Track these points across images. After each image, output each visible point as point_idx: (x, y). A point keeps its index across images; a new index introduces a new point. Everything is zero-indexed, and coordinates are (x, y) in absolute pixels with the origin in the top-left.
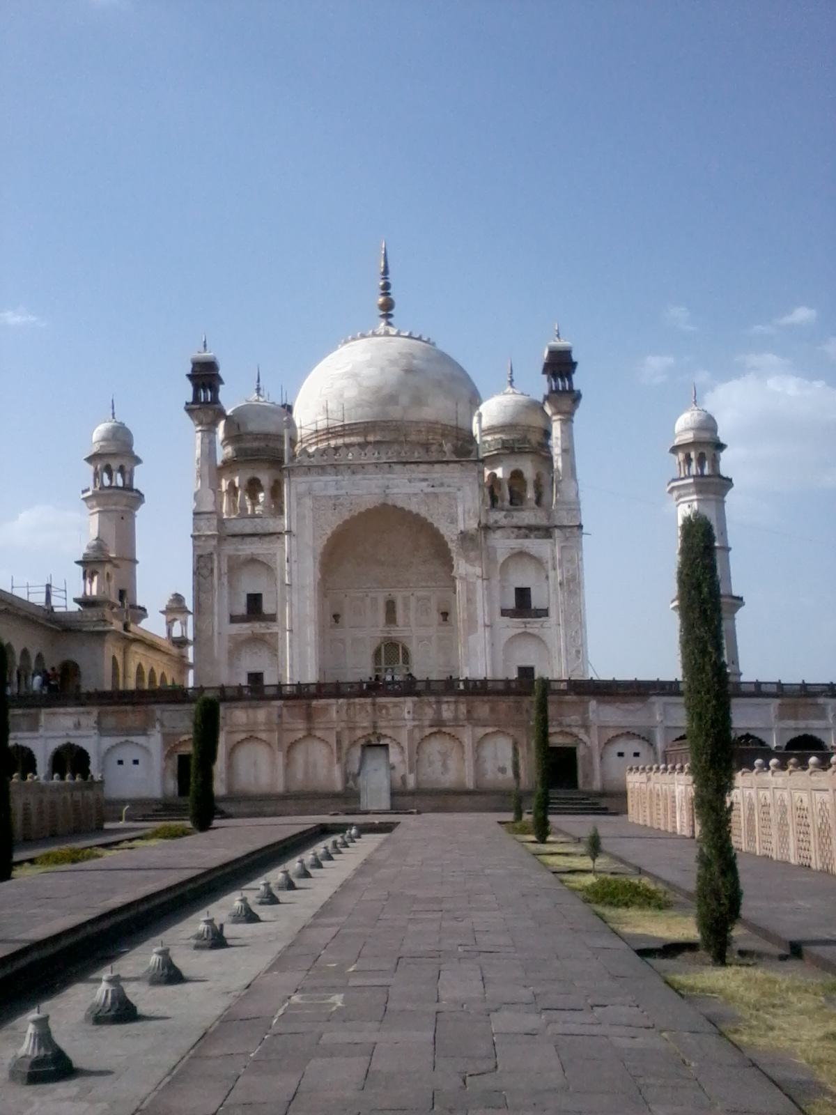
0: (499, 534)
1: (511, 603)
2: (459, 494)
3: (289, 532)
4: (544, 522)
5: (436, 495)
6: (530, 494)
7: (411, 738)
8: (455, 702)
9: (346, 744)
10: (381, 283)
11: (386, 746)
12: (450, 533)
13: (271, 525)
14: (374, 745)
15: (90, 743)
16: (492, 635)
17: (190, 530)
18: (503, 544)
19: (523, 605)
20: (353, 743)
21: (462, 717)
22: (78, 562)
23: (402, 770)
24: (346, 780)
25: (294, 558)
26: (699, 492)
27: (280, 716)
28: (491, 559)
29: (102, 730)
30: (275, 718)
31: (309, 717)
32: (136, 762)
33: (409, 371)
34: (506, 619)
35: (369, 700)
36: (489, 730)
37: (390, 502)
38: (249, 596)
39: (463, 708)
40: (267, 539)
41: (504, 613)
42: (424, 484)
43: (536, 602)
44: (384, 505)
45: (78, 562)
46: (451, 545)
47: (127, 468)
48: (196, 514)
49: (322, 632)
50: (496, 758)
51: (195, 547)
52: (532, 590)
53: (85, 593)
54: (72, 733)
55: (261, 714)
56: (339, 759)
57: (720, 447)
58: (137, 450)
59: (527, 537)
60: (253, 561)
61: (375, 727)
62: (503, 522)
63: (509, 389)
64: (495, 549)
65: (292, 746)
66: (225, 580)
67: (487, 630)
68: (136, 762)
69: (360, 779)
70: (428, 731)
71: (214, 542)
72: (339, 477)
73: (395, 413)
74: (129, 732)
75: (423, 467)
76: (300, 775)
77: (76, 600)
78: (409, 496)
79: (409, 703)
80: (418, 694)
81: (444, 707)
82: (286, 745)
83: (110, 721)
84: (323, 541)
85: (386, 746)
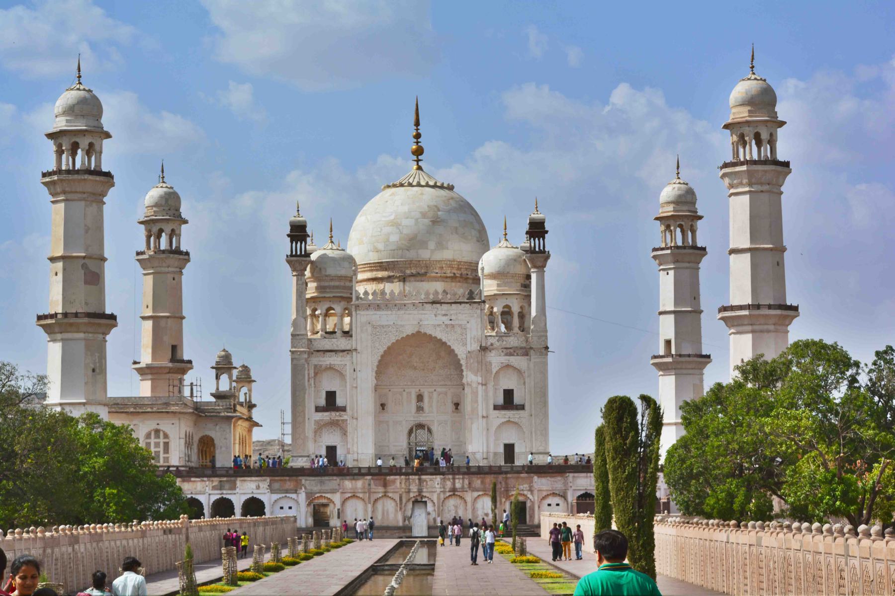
0: (493, 353)
1: (500, 400)
2: (468, 326)
3: (356, 350)
4: (524, 345)
5: (453, 326)
6: (516, 322)
7: (439, 498)
8: (463, 479)
9: (404, 501)
10: (414, 147)
11: (425, 502)
12: (461, 352)
13: (341, 343)
14: (419, 501)
15: (267, 498)
16: (487, 424)
17: (290, 348)
18: (496, 360)
19: (508, 401)
20: (409, 500)
21: (466, 486)
22: (213, 368)
23: (433, 515)
24: (404, 521)
25: (358, 369)
26: (676, 261)
27: (369, 485)
28: (489, 371)
29: (272, 491)
30: (367, 485)
31: (385, 485)
32: (290, 508)
33: (435, 222)
34: (497, 412)
35: (417, 477)
36: (481, 493)
37: (422, 331)
38: (327, 392)
39: (466, 482)
40: (341, 354)
41: (496, 408)
42: (444, 318)
43: (517, 400)
44: (419, 332)
45: (213, 368)
46: (463, 362)
47: (177, 232)
48: (292, 335)
49: (376, 416)
50: (483, 508)
51: (292, 360)
52: (515, 392)
53: (218, 389)
54: (255, 491)
55: (360, 483)
56: (401, 509)
57: (700, 218)
58: (185, 212)
59: (511, 355)
60: (330, 368)
61: (420, 491)
62: (497, 344)
63: (504, 243)
64: (490, 363)
65: (376, 500)
66: (312, 382)
67: (485, 420)
68: (290, 508)
69: (412, 520)
70: (448, 494)
71: (306, 356)
72: (390, 312)
73: (425, 255)
74: (287, 491)
75: (445, 307)
76: (380, 517)
77: (212, 395)
78: (435, 326)
79: (438, 478)
80: (443, 474)
81: (457, 481)
82: (372, 500)
83: (276, 486)
84: (377, 357)
85: (425, 502)
